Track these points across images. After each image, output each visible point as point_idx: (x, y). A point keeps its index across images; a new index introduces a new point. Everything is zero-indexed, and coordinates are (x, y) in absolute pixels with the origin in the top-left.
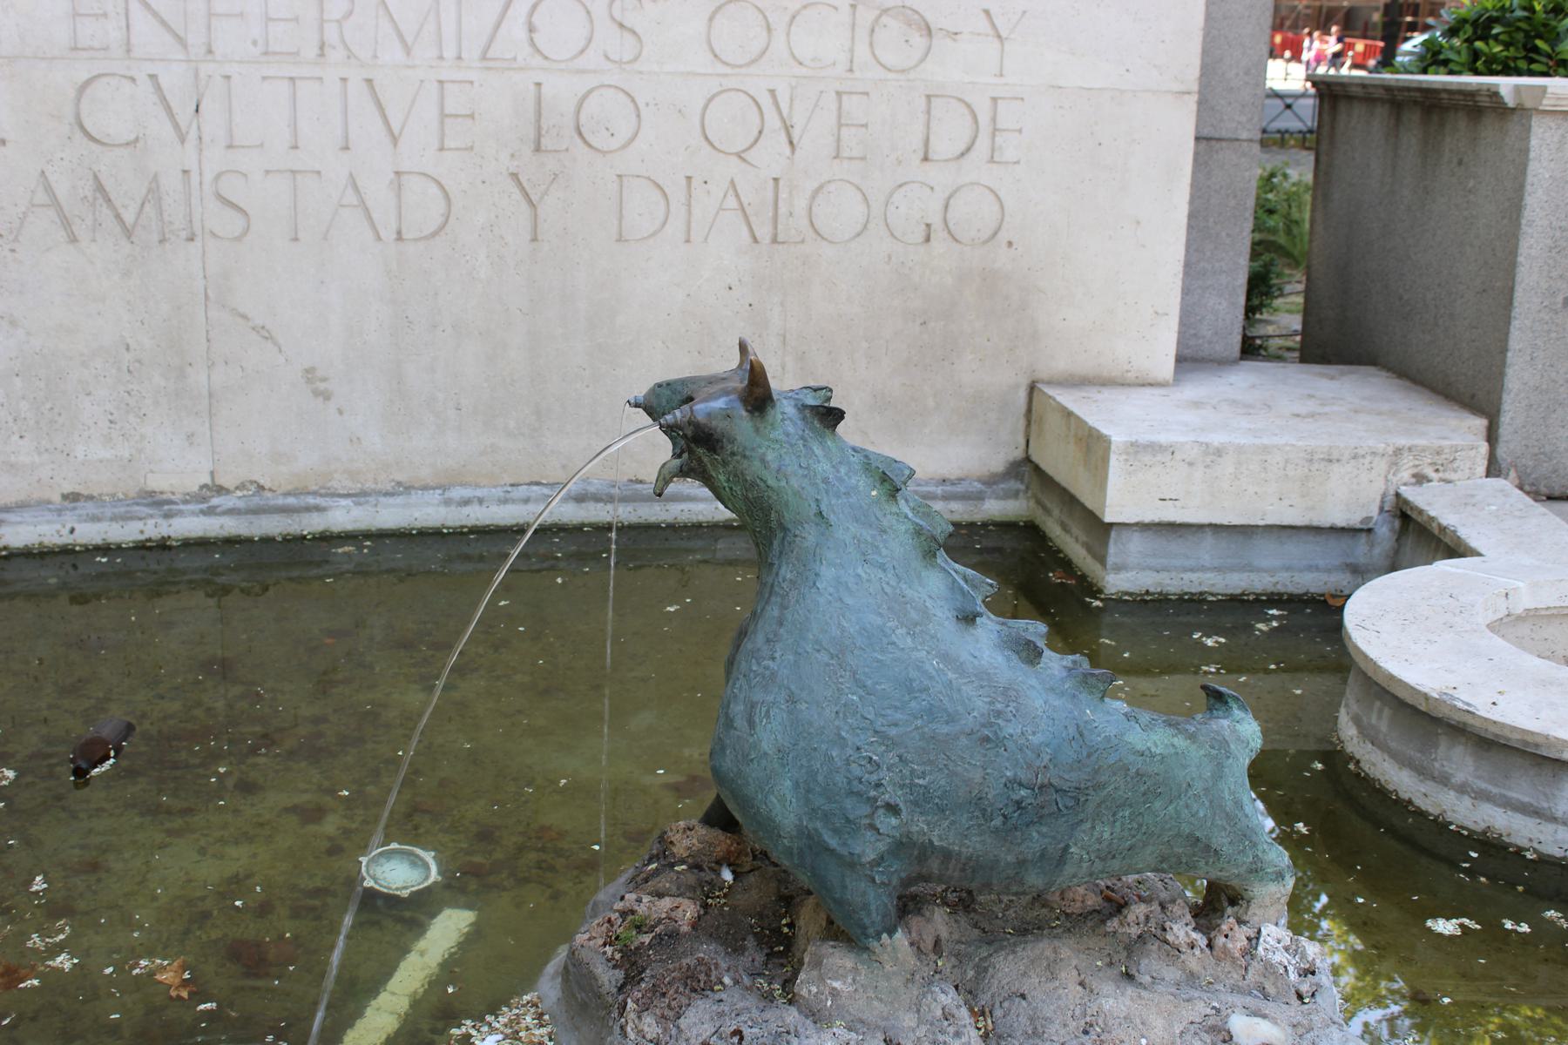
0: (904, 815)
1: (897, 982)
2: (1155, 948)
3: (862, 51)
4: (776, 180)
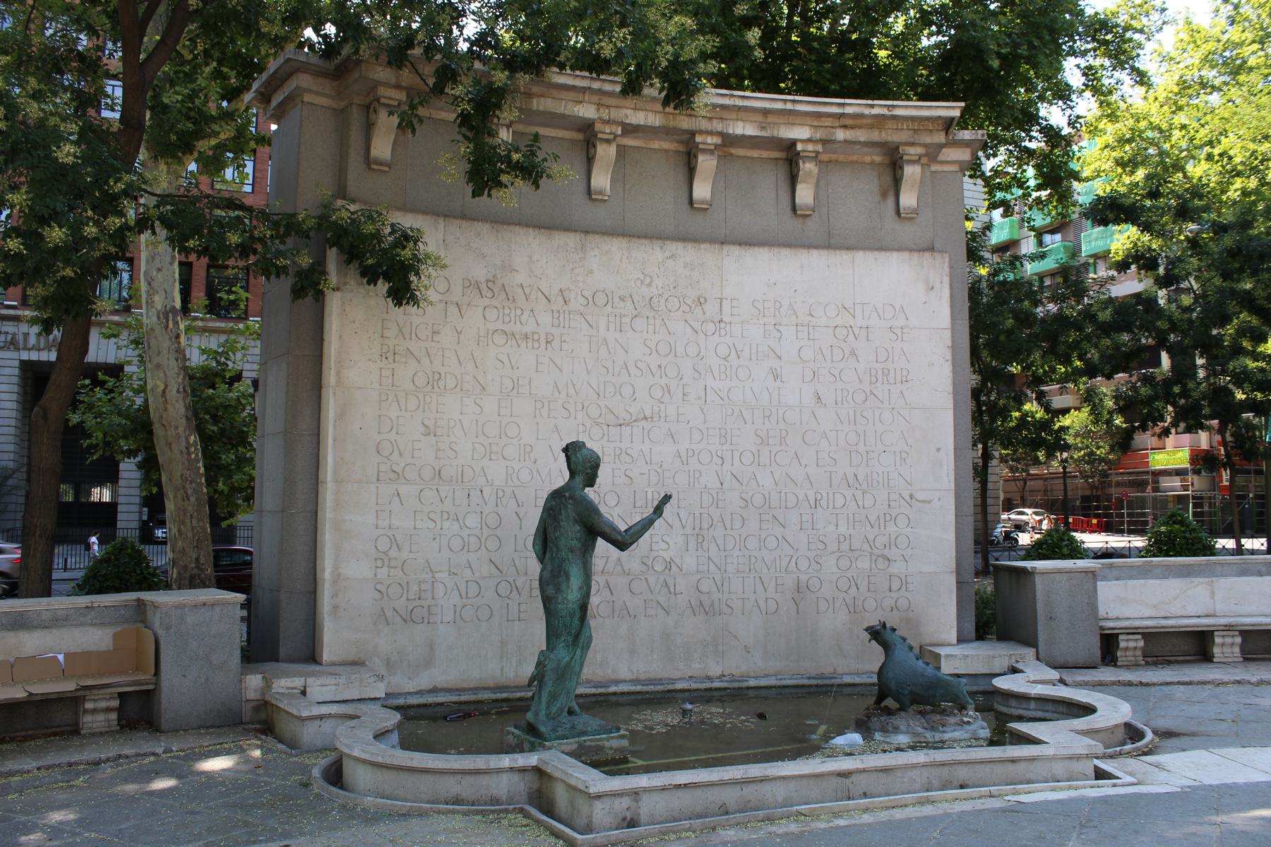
3: (874, 566)
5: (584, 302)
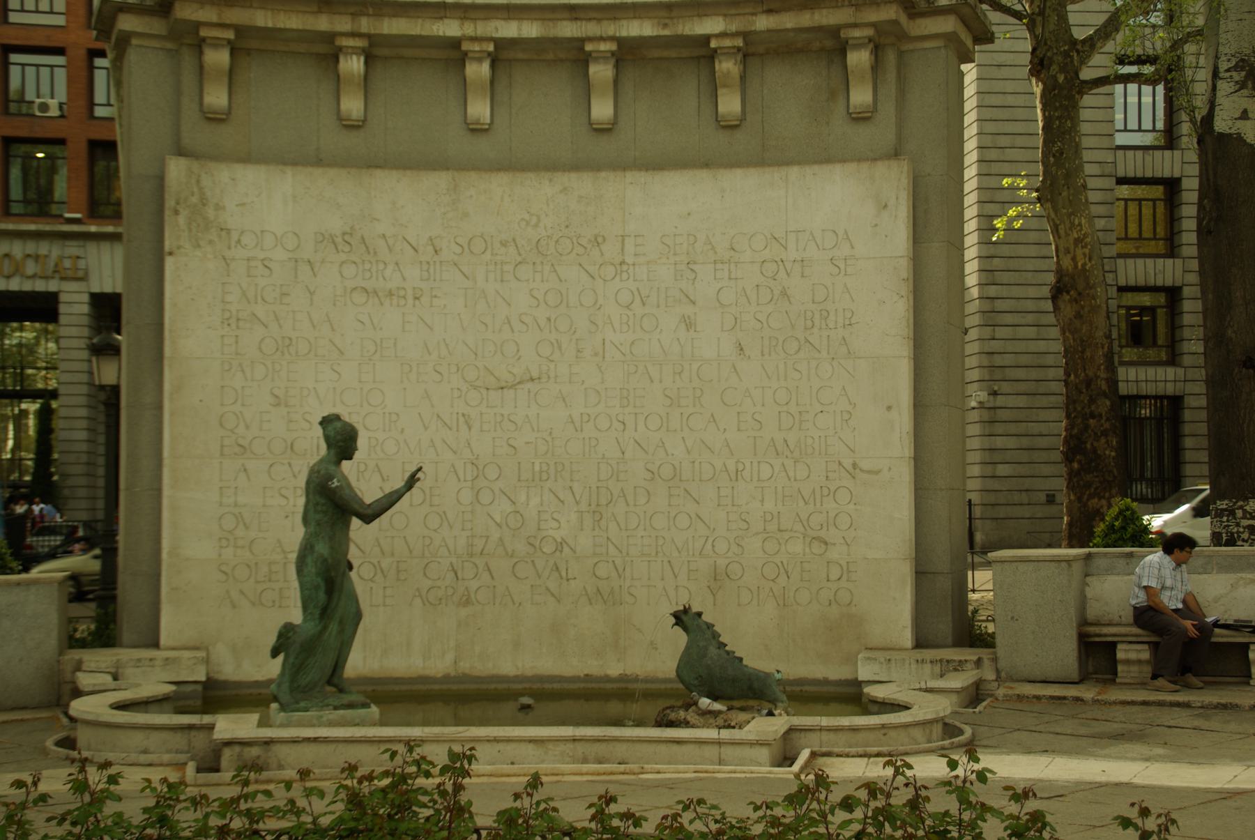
3: (807, 550)
5: (458, 250)
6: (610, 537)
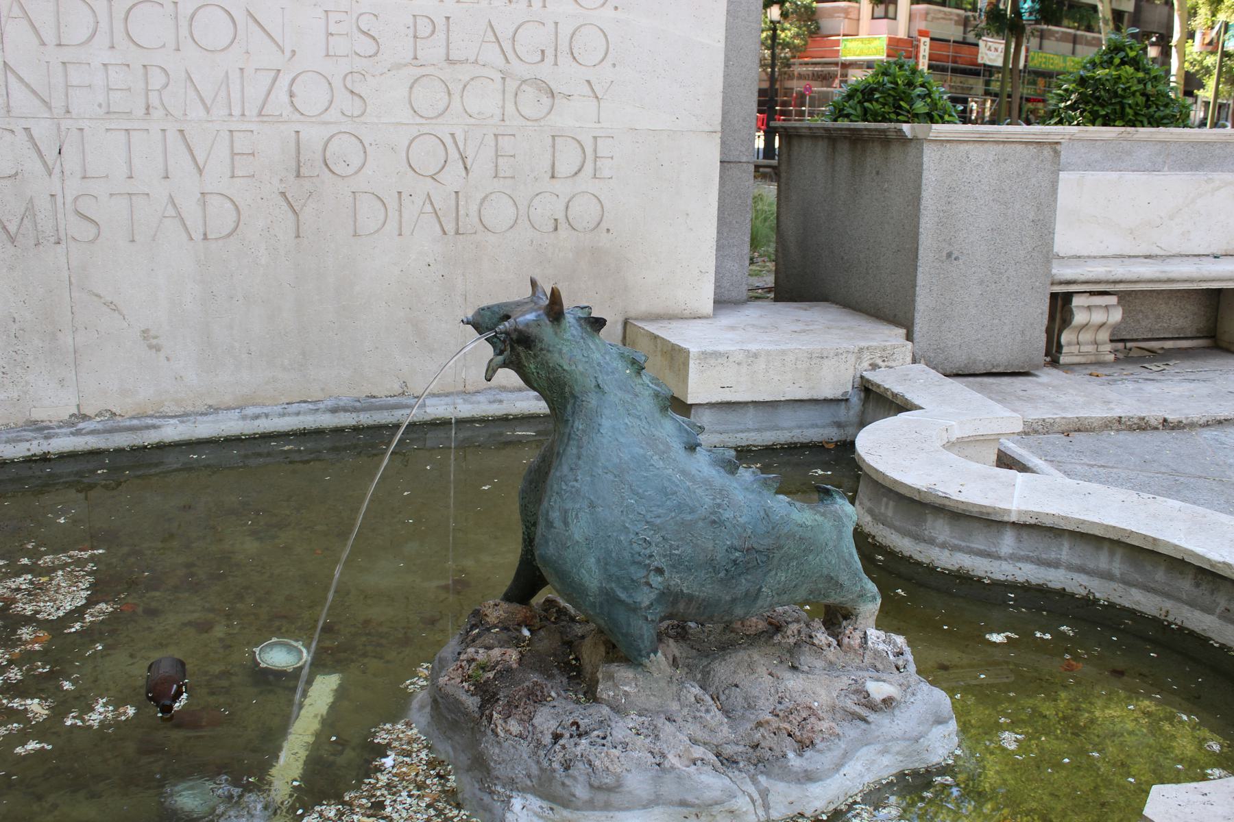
0: (667, 574)
1: (663, 684)
2: (807, 649)
3: (510, 107)
4: (456, 192)
6: (11, 64)
